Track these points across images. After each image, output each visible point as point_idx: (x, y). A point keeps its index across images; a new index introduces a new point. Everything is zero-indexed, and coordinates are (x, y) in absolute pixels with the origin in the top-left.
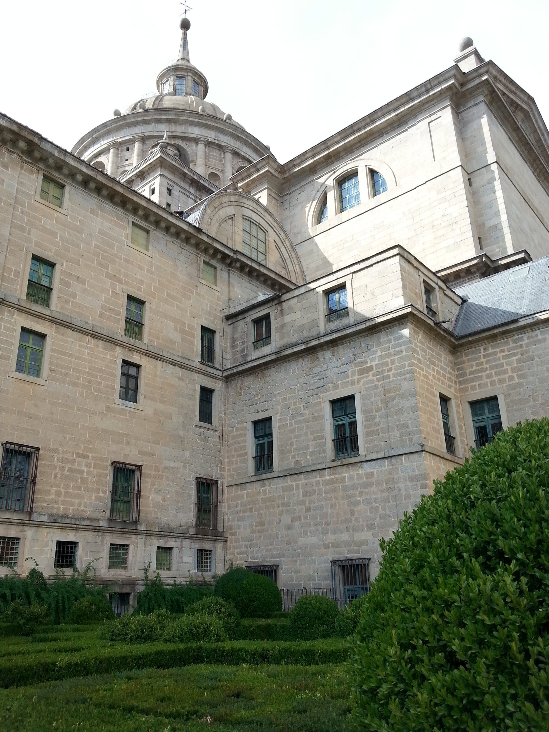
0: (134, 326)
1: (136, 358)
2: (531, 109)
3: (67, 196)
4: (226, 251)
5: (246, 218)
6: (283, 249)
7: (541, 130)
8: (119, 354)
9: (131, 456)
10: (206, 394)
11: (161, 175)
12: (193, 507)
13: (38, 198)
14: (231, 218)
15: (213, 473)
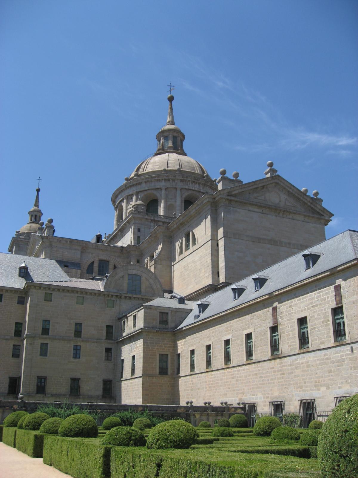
0: (78, 333)
1: (79, 344)
2: (279, 179)
3: (53, 296)
4: (116, 294)
5: (129, 275)
6: (151, 281)
7: (288, 187)
8: (72, 345)
9: (77, 375)
10: (108, 350)
11: (134, 223)
12: (101, 389)
13: (44, 301)
14: (122, 277)
15: (110, 377)
